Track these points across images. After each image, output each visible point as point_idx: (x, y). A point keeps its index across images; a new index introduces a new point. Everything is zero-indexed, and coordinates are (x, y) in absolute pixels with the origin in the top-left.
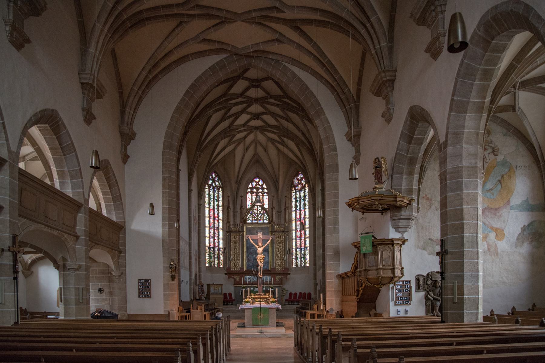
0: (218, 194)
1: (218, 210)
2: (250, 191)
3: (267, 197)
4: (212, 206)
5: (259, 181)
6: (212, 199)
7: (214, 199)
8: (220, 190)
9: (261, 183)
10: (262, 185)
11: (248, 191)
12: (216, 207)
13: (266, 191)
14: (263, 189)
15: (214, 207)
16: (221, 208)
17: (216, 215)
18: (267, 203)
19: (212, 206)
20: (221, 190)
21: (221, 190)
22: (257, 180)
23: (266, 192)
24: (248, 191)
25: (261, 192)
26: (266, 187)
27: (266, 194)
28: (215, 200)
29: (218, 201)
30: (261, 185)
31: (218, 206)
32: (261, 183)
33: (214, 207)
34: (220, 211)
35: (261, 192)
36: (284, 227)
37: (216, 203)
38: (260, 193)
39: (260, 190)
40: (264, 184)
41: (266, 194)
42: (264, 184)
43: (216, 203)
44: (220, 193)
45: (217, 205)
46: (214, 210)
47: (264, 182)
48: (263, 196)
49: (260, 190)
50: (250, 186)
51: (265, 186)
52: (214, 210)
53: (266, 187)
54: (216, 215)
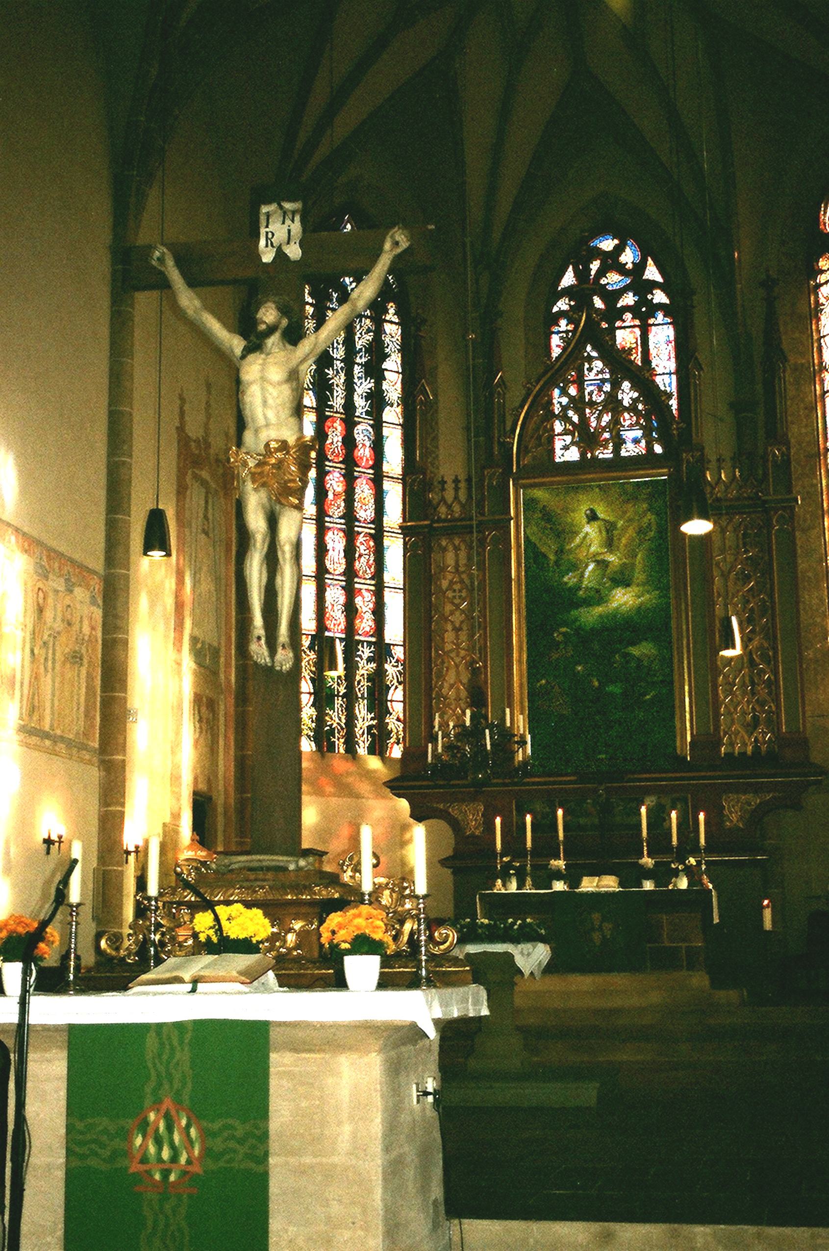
0: (379, 331)
1: (378, 426)
2: (565, 307)
3: (669, 332)
4: (338, 401)
5: (619, 250)
6: (339, 365)
7: (349, 362)
8: (386, 311)
9: (628, 257)
10: (640, 267)
11: (555, 309)
12: (360, 402)
13: (659, 297)
14: (643, 288)
15: (349, 406)
16: (392, 415)
17: (364, 452)
18: (672, 366)
19: (338, 401)
20: (392, 311)
21: (392, 311)
22: (608, 244)
23: (661, 306)
24: (555, 309)
25: (633, 310)
26: (659, 278)
27: (660, 316)
28: (357, 369)
29: (375, 371)
30: (630, 266)
31: (377, 400)
32: (628, 257)
33: (349, 406)
34: (386, 431)
35: (633, 310)
36: (765, 474)
37: (363, 386)
38: (628, 316)
39: (629, 299)
40: (650, 261)
41: (660, 316)
42: (650, 261)
43: (363, 386)
44: (388, 327)
45: (369, 396)
46: (350, 423)
47: (646, 252)
48: (645, 331)
49: (629, 299)
50: (568, 279)
51: (652, 273)
52: (350, 423)
53: (659, 278)
54: (364, 452)
